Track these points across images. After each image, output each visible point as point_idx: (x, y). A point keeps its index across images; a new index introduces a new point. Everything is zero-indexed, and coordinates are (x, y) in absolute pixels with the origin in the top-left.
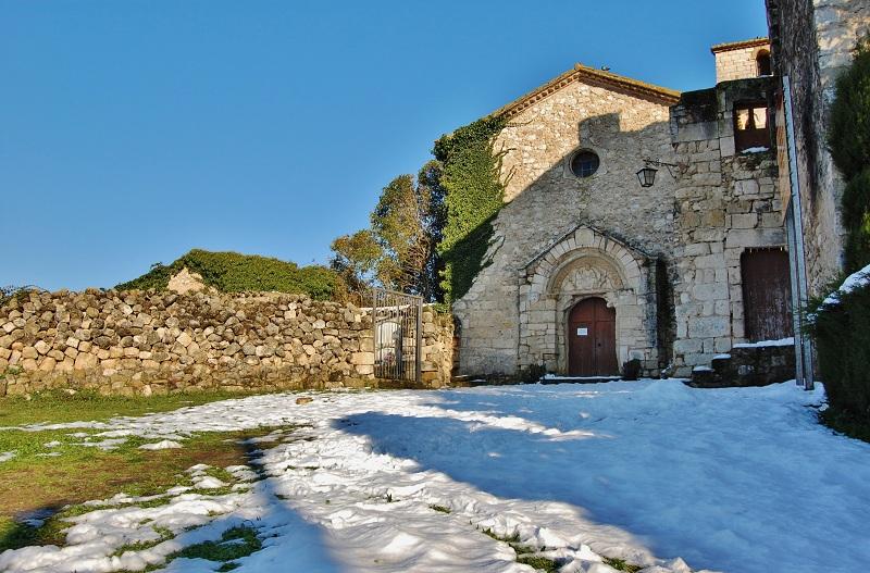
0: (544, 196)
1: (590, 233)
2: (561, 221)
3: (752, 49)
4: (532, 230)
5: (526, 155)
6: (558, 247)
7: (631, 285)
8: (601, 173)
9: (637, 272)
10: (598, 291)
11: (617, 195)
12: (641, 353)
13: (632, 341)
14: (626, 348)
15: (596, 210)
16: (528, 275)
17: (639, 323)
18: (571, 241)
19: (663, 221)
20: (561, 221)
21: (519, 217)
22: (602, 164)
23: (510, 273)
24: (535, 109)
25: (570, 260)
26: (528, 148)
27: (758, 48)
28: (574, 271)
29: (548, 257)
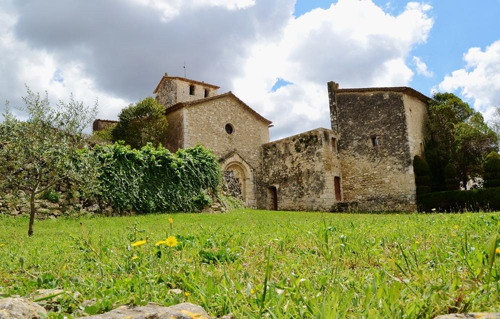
5: (210, 119)
8: (235, 134)
9: (250, 173)
12: (252, 201)
15: (234, 147)
17: (251, 190)
21: (209, 144)
24: (213, 102)
25: (231, 165)
26: (211, 117)
29: (225, 162)
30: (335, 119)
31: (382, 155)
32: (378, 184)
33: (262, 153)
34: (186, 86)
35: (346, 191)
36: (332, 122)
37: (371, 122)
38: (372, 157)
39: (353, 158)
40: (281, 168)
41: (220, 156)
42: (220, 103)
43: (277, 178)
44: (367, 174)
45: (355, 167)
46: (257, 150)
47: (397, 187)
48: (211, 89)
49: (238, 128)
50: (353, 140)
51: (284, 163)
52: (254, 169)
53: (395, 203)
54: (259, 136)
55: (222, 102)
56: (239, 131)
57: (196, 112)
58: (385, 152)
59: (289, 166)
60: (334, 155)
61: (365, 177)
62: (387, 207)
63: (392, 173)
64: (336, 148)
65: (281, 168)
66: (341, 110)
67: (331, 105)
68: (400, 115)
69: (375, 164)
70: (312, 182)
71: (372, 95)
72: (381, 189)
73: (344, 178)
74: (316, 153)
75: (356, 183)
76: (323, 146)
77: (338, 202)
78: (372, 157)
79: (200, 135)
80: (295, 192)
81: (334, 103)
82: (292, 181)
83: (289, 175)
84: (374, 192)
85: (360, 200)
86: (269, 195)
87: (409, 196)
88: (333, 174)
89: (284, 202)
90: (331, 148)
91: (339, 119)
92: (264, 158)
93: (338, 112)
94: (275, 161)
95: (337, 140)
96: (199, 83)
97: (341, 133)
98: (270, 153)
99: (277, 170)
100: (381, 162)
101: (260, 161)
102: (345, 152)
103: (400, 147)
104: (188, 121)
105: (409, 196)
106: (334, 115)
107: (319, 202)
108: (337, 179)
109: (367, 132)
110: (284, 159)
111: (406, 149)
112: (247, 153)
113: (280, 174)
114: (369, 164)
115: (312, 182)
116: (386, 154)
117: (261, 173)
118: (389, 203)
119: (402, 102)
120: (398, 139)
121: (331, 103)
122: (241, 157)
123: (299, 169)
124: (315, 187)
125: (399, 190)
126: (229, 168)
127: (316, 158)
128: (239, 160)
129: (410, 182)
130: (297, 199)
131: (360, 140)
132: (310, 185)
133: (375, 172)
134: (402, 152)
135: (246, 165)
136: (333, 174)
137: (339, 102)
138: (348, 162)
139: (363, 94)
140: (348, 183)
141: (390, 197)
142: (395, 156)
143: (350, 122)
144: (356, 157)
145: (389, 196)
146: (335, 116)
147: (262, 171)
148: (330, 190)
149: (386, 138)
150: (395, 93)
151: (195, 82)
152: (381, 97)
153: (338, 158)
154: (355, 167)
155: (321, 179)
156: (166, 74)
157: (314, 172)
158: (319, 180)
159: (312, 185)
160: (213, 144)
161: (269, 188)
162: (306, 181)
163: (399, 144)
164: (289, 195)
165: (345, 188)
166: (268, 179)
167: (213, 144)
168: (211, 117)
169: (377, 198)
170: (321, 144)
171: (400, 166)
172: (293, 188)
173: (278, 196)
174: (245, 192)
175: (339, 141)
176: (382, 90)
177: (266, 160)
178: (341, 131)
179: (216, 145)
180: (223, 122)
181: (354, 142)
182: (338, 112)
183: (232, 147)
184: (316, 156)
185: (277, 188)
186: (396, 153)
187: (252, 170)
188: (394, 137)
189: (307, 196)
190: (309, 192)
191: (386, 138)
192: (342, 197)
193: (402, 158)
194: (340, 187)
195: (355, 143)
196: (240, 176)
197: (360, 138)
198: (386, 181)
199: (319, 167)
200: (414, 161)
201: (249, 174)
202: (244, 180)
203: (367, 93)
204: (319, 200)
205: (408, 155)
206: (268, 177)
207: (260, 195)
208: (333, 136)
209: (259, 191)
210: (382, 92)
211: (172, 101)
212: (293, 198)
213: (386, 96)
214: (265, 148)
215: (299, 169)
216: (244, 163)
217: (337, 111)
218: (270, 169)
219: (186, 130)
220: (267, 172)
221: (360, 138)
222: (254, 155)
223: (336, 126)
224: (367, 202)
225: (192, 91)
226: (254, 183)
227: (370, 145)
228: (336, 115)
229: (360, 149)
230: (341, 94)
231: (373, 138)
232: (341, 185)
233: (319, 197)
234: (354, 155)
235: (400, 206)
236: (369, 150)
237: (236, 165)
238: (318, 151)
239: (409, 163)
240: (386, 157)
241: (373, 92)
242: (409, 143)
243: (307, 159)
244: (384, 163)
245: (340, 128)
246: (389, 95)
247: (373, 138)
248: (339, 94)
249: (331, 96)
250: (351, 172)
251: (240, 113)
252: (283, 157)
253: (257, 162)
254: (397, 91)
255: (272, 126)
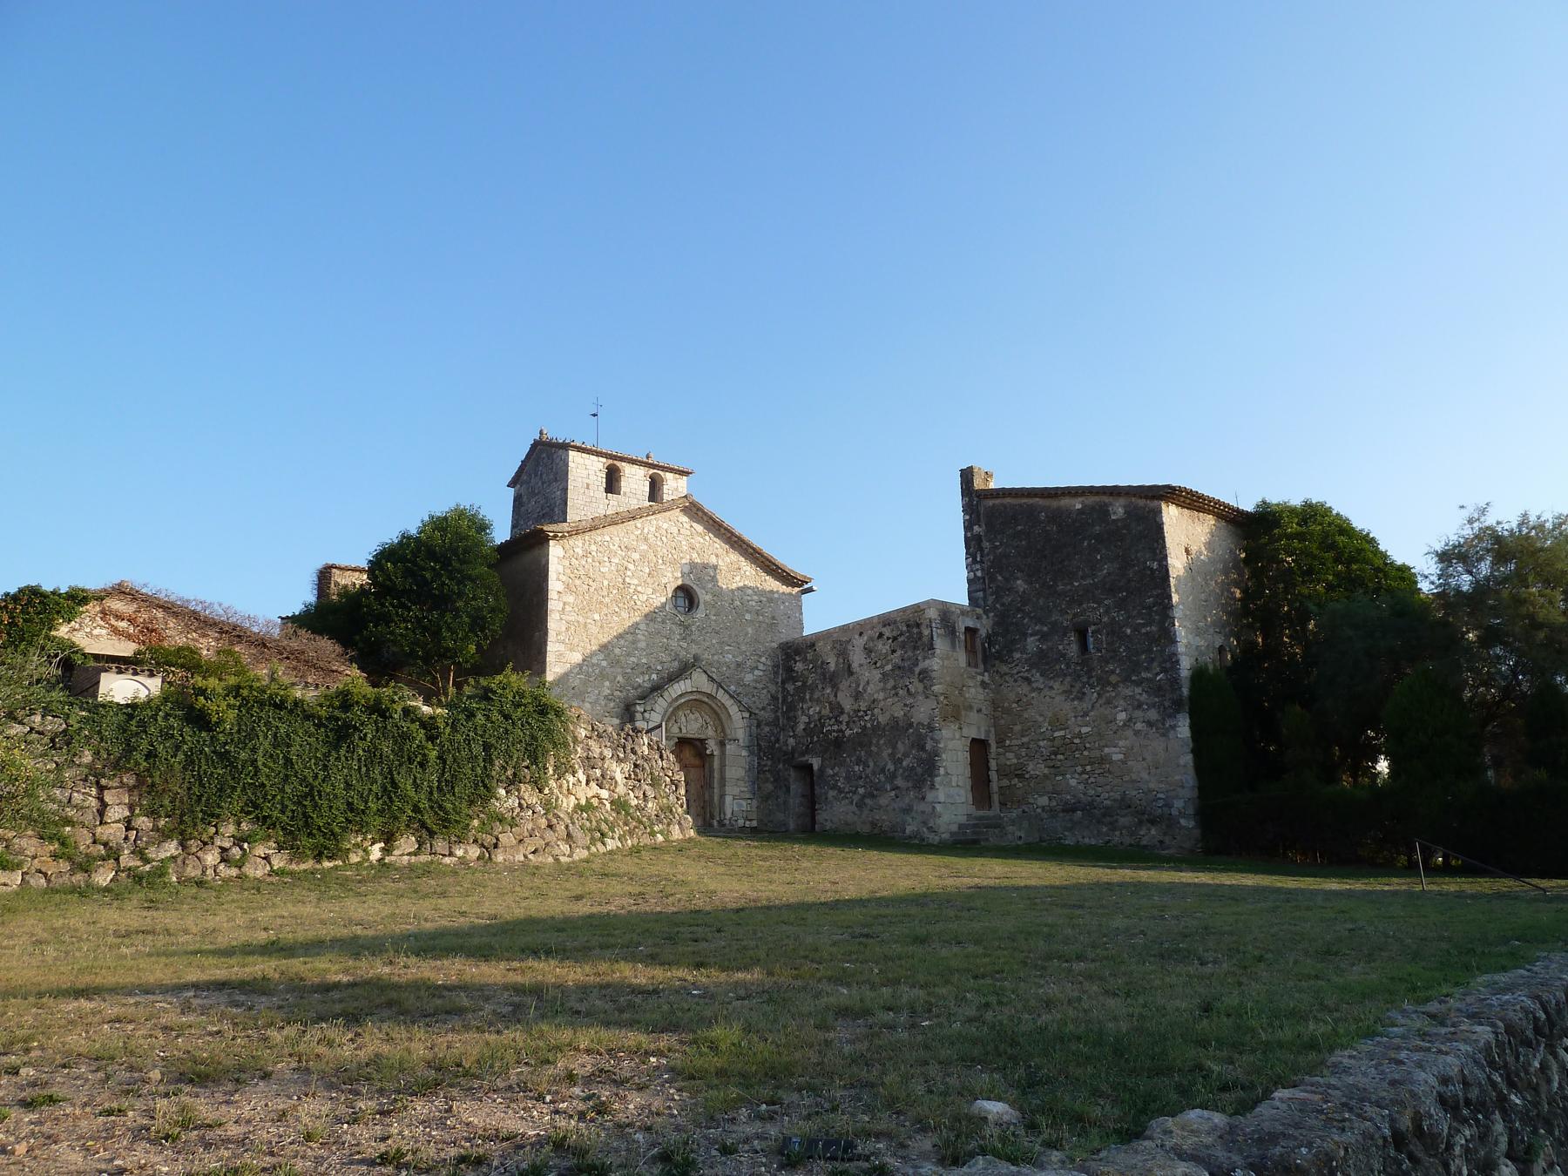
0: (647, 624)
1: (704, 677)
2: (664, 657)
3: (604, 460)
4: (635, 660)
5: (629, 573)
6: (676, 686)
7: (733, 736)
8: (700, 614)
10: (703, 737)
11: (714, 641)
12: (744, 803)
13: (736, 791)
14: (731, 797)
15: (694, 649)
16: (645, 711)
17: (741, 773)
18: (688, 681)
19: (751, 675)
20: (664, 657)
22: (702, 606)
23: (612, 705)
25: (683, 701)
27: (610, 462)
28: (680, 713)
29: (666, 694)
30: (979, 574)
31: (1104, 682)
32: (1091, 764)
33: (778, 666)
34: (597, 466)
35: (1005, 782)
36: (969, 581)
37: (1076, 584)
38: (1078, 685)
39: (1025, 689)
40: (826, 712)
41: (654, 676)
42: (658, 528)
43: (815, 739)
44: (1062, 733)
45: (1031, 713)
46: (763, 659)
47: (1145, 775)
48: (669, 476)
49: (708, 598)
50: (1025, 635)
51: (836, 696)
52: (751, 713)
53: (1141, 822)
54: (773, 618)
55: (665, 526)
56: (714, 606)
57: (587, 554)
58: (1113, 672)
59: (848, 704)
60: (973, 678)
61: (1057, 743)
62: (1117, 833)
63: (1129, 733)
64: (980, 656)
65: (826, 712)
66: (996, 547)
67: (969, 535)
68: (1155, 566)
69: (1086, 705)
70: (906, 755)
71: (1079, 506)
72: (1101, 780)
73: (1000, 742)
74: (917, 670)
75: (1032, 758)
76: (938, 651)
77: (981, 813)
78: (1078, 685)
79: (597, 617)
80: (861, 782)
81: (976, 528)
82: (855, 750)
83: (848, 732)
84: (1081, 787)
85: (1043, 808)
86: (796, 787)
87: (1179, 804)
88: (966, 732)
89: (836, 812)
90: (962, 657)
91: (989, 573)
92: (783, 682)
93: (988, 555)
94: (813, 689)
95: (983, 632)
96: (633, 462)
97: (996, 616)
98: (799, 666)
99: (816, 717)
100: (1100, 702)
101: (773, 688)
102: (1004, 668)
103: (1153, 660)
104: (564, 578)
105: (1179, 804)
106: (975, 561)
107: (923, 812)
108: (978, 747)
109: (1063, 612)
110: (835, 687)
111: (1168, 665)
112: (732, 666)
113: (823, 726)
114: (1067, 706)
115: (906, 755)
116: (1113, 679)
117: (775, 723)
118: (1123, 821)
119: (1159, 529)
120: (1147, 633)
121: (968, 527)
122: (713, 680)
123: (873, 715)
124: (913, 768)
125: (1152, 786)
126: (678, 708)
127: (917, 686)
128: (707, 687)
129: (1182, 762)
130: (868, 801)
131: (1044, 637)
132: (900, 761)
133: (1084, 730)
134: (1157, 674)
135: (728, 702)
136: (966, 732)
137: (990, 527)
138: (1012, 696)
139: (1054, 503)
140: (1011, 759)
141: (1125, 804)
142: (1138, 683)
143: (1019, 582)
144: (1034, 685)
145: (1123, 799)
146: (978, 566)
147: (777, 718)
148: (954, 779)
149: (1114, 630)
150: (1141, 502)
151: (622, 459)
152: (1103, 511)
153: (984, 684)
154: (1031, 713)
155: (928, 747)
156: (541, 433)
157: (911, 725)
158: (923, 748)
159: (905, 763)
160: (634, 642)
161: (795, 767)
162: (890, 751)
163: (1150, 651)
164: (847, 790)
165: (1003, 772)
166: (791, 741)
167: (634, 642)
168: (631, 566)
169: (1091, 804)
170: (931, 647)
171: (1153, 715)
172: (856, 768)
173: (817, 790)
174: (723, 779)
175: (988, 636)
176: (1104, 493)
177: (790, 687)
178: (993, 609)
179: (642, 645)
180: (664, 581)
181: (1030, 640)
182: (988, 555)
183: (688, 651)
184: (916, 681)
185: (816, 767)
186: (1144, 675)
187: (746, 715)
188: (1136, 629)
189: (893, 793)
190: (899, 782)
191: (1114, 630)
192: (996, 798)
193: (1158, 690)
194: (989, 769)
195: (1032, 643)
196: (710, 732)
197: (1045, 629)
198: (1116, 757)
199: (923, 711)
200: (1191, 698)
201: (738, 724)
202: (722, 744)
203: (1065, 502)
204: (922, 807)
205: (1175, 682)
206: (794, 736)
207: (770, 787)
208: (971, 624)
209: (768, 775)
210: (1106, 499)
211: (556, 509)
212: (856, 798)
213: (1118, 510)
214: (787, 654)
215: (873, 715)
216: (721, 695)
217: (986, 551)
218: (800, 713)
219: (554, 605)
220: (793, 720)
221: (1045, 629)
222: (756, 672)
223: (980, 594)
224: (1061, 815)
225: (612, 482)
226: (751, 753)
227: (1073, 650)
228: (982, 562)
229: (1044, 662)
230: (997, 501)
231: (1082, 634)
232: (993, 764)
233: (923, 798)
234: (1027, 679)
235: (1153, 832)
236: (1068, 666)
237: (697, 703)
238: (922, 665)
239: (1178, 705)
240: (1115, 686)
241: (1080, 499)
242: (1181, 649)
243: (895, 687)
244: (1108, 702)
245: (991, 599)
246: (1124, 507)
247: (1082, 634)
248: (990, 503)
249: (968, 508)
250: (1017, 728)
251: (717, 556)
252: (832, 680)
253: (765, 691)
254: (1146, 497)
255: (810, 590)
